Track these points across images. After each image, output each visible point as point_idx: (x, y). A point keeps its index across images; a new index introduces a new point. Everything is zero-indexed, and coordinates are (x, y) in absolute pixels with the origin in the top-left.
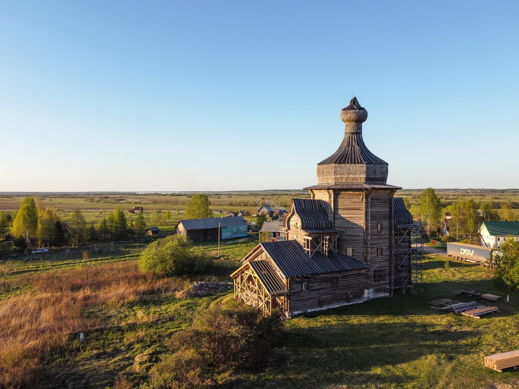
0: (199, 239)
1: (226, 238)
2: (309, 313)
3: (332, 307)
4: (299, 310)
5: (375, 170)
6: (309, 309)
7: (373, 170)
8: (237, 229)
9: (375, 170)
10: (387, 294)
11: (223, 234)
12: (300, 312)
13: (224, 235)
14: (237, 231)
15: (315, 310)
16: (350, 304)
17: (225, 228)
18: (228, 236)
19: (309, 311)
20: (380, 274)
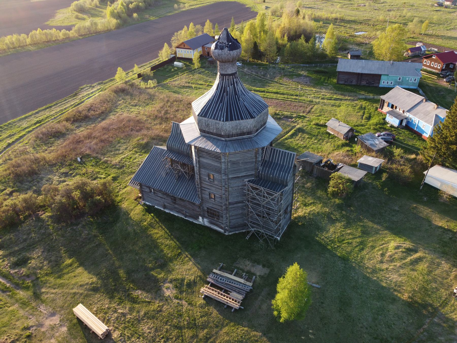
0: (352, 82)
1: (386, 86)
2: (156, 208)
3: (172, 213)
4: (151, 203)
5: (208, 125)
6: (156, 205)
7: (205, 124)
8: (403, 79)
9: (208, 125)
10: (222, 231)
11: (382, 82)
12: (150, 204)
13: (384, 83)
14: (402, 81)
15: (160, 208)
16: (186, 219)
17: (386, 77)
18: (389, 85)
19: (156, 207)
20: (214, 213)
